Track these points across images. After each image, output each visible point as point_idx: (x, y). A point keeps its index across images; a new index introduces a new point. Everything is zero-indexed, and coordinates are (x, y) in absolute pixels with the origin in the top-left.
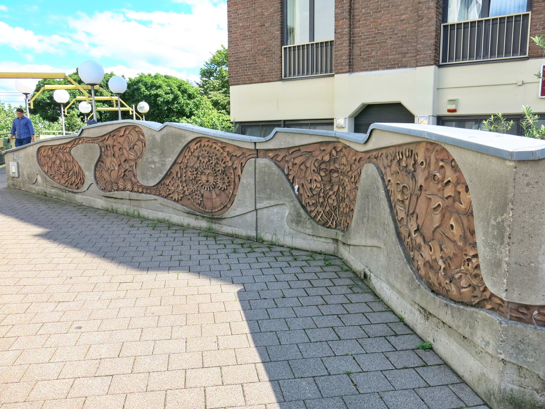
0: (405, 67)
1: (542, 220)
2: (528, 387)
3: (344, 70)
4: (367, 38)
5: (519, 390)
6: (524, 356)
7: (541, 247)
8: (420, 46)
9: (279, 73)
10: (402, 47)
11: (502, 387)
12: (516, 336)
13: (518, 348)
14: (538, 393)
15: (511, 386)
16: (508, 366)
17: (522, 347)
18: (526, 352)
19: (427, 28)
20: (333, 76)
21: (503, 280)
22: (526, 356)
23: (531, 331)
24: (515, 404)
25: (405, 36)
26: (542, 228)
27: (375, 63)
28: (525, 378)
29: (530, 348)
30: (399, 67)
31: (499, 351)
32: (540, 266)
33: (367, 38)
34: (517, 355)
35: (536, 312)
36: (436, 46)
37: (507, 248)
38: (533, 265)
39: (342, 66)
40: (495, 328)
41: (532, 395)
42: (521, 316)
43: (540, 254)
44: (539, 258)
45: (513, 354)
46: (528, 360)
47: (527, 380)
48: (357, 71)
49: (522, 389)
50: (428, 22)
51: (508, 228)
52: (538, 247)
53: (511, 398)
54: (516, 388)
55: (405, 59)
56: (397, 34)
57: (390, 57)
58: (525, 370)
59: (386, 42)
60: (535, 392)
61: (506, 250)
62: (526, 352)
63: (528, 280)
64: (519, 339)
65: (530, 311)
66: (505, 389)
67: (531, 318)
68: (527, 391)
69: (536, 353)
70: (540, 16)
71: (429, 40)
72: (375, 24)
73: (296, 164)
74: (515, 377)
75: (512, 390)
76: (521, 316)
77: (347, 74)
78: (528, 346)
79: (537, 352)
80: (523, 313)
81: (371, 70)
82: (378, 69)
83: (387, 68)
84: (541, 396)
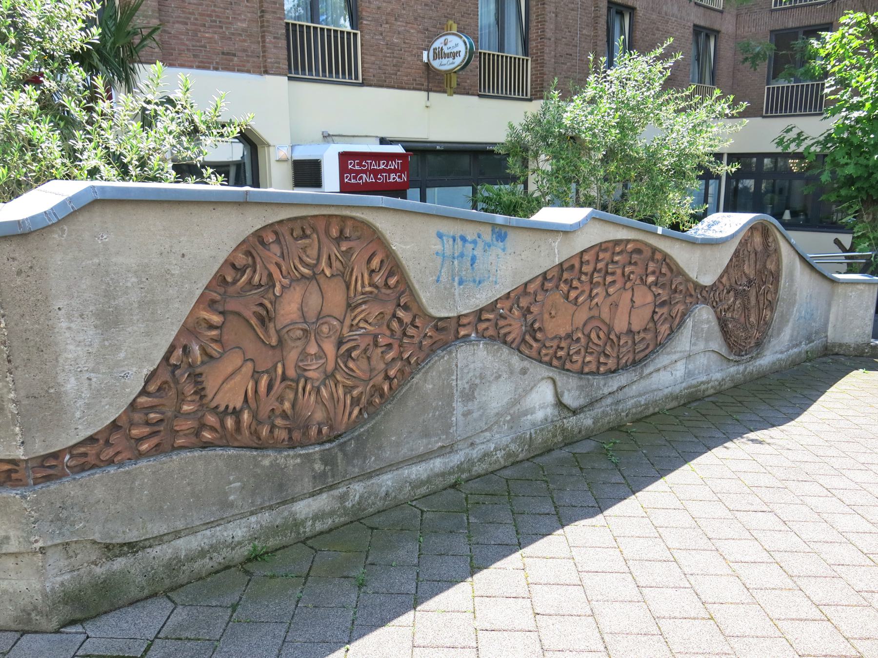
1: (50, 323)
2: (82, 565)
5: (72, 577)
6: (71, 525)
7: (58, 362)
11: (48, 590)
12: (52, 503)
13: (60, 519)
14: (96, 565)
15: (59, 579)
16: (49, 553)
17: (64, 514)
18: (72, 519)
21: (13, 430)
22: (72, 525)
23: (71, 486)
24: (72, 600)
26: (53, 333)
28: (76, 555)
29: (75, 510)
31: (32, 539)
32: (63, 389)
34: (60, 529)
35: (67, 457)
37: (8, 379)
38: (52, 391)
40: (16, 508)
41: (90, 572)
42: (51, 472)
43: (59, 372)
44: (59, 377)
45: (54, 532)
46: (77, 527)
47: (79, 556)
49: (76, 573)
51: (2, 347)
52: (54, 362)
53: (65, 595)
54: (67, 577)
58: (73, 545)
60: (93, 566)
61: (8, 382)
62: (72, 519)
63: (51, 415)
64: (58, 505)
65: (60, 459)
66: (53, 589)
67: (63, 469)
68: (82, 571)
69: (84, 512)
73: (588, 261)
74: (63, 563)
75: (62, 584)
76: (51, 472)
78: (72, 508)
79: (86, 510)
80: (50, 467)
84: (101, 567)
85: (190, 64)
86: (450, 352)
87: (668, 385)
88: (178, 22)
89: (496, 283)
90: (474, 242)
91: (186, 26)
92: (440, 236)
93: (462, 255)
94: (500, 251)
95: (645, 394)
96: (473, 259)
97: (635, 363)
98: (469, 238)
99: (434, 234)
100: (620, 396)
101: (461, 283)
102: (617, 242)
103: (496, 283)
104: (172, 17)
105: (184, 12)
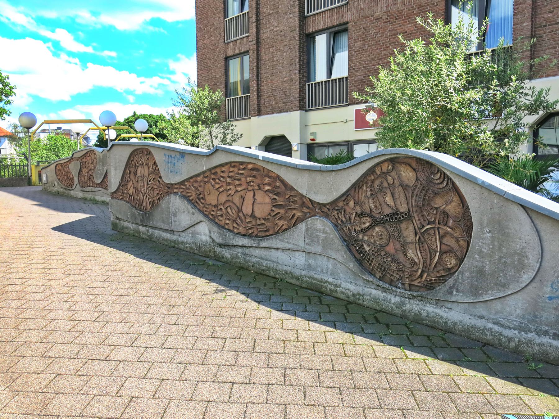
0: (287, 112)
3: (255, 115)
4: (268, 93)
8: (292, 98)
9: (225, 116)
10: (285, 99)
19: (295, 87)
20: (250, 118)
25: (286, 92)
27: (272, 109)
30: (284, 112)
33: (268, 93)
36: (300, 97)
39: (254, 111)
48: (263, 115)
50: (295, 83)
55: (287, 106)
56: (282, 90)
57: (280, 105)
59: (277, 95)
70: (352, 78)
71: (296, 94)
72: (271, 83)
77: (257, 117)
81: (270, 114)
82: (273, 113)
83: (278, 113)
85: (554, 73)
86: (169, 196)
87: (287, 265)
88: (549, 48)
89: (182, 174)
90: (174, 158)
91: (555, 49)
92: (165, 155)
93: (171, 162)
94: (182, 162)
95: (265, 260)
96: (174, 164)
97: (257, 236)
98: (173, 156)
99: (163, 154)
100: (248, 251)
101: (171, 172)
102: (242, 163)
103: (182, 174)
104: (545, 46)
105: (555, 41)
